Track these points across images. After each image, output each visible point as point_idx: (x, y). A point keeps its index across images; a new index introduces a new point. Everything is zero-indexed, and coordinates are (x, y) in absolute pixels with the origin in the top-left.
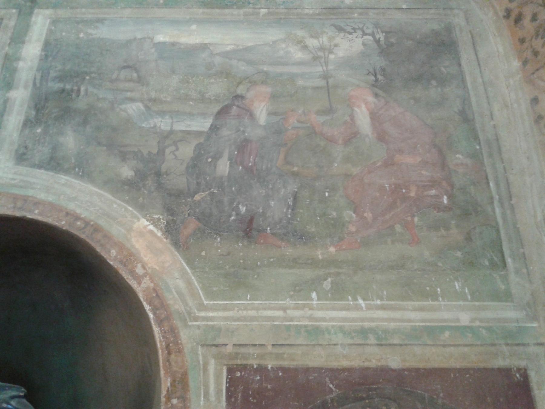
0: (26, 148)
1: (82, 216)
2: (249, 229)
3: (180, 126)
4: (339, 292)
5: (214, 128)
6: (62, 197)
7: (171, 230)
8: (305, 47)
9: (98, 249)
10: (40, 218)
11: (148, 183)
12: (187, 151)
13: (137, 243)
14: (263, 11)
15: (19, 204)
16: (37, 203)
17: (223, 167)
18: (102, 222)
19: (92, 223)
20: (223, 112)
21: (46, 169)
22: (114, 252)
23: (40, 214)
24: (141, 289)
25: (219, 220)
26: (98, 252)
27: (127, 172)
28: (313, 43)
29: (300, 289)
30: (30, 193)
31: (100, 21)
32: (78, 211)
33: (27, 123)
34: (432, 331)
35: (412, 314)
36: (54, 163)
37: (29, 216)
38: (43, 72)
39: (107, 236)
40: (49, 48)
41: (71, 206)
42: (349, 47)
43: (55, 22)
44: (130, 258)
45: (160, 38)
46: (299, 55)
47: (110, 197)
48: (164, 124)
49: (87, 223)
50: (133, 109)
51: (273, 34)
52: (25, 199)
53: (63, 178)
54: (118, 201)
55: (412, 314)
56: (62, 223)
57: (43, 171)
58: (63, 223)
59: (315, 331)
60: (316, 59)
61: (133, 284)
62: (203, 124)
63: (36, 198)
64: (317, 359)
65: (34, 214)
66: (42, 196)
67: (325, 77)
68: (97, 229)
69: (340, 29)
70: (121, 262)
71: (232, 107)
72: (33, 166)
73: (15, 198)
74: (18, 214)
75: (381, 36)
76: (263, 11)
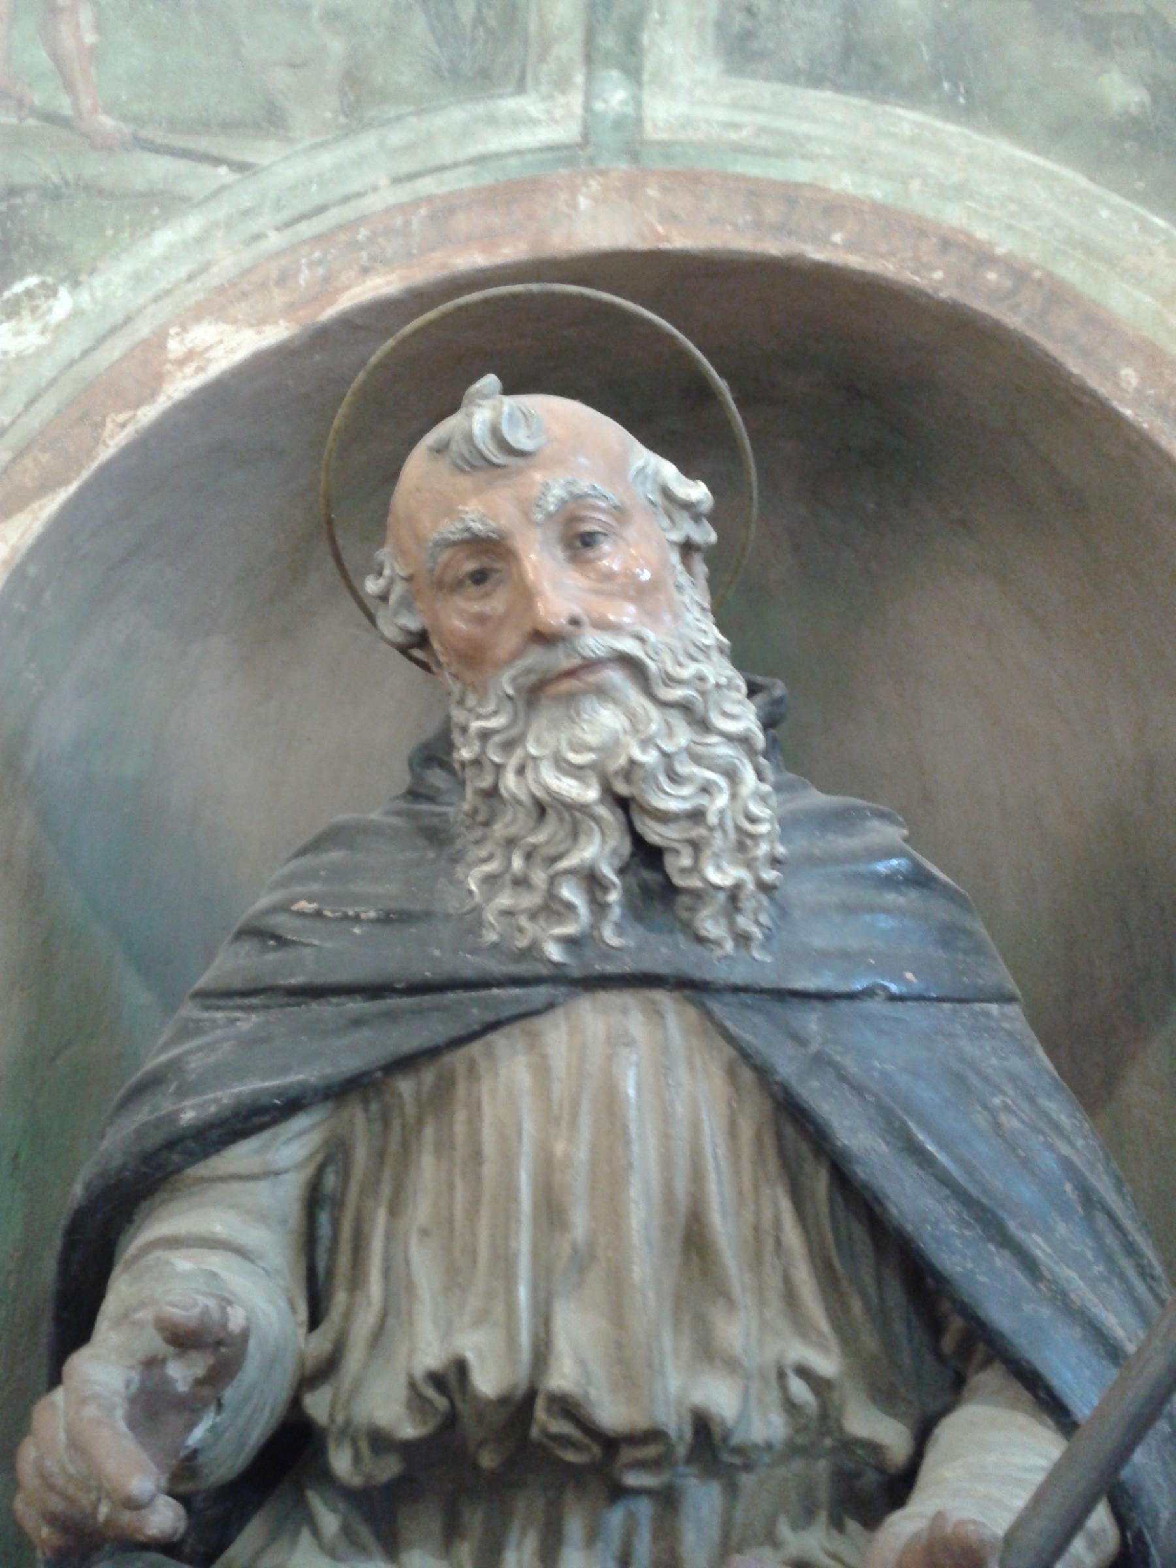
0: (750, 12)
1: (1000, 251)
6: (915, 185)
9: (1075, 366)
10: (855, 261)
15: (772, 213)
16: (835, 209)
18: (1070, 272)
19: (1037, 274)
21: (838, 88)
22: (1130, 376)
23: (851, 246)
26: (1071, 375)
30: (801, 172)
32: (982, 233)
37: (816, 254)
39: (1096, 320)
41: (954, 216)
47: (1083, 182)
49: (1020, 274)
52: (790, 194)
53: (907, 118)
54: (1116, 199)
56: (935, 279)
57: (828, 94)
58: (938, 275)
63: (826, 190)
65: (832, 249)
66: (845, 183)
68: (1057, 295)
70: (1161, 408)
72: (792, 76)
73: (755, 192)
74: (774, 248)
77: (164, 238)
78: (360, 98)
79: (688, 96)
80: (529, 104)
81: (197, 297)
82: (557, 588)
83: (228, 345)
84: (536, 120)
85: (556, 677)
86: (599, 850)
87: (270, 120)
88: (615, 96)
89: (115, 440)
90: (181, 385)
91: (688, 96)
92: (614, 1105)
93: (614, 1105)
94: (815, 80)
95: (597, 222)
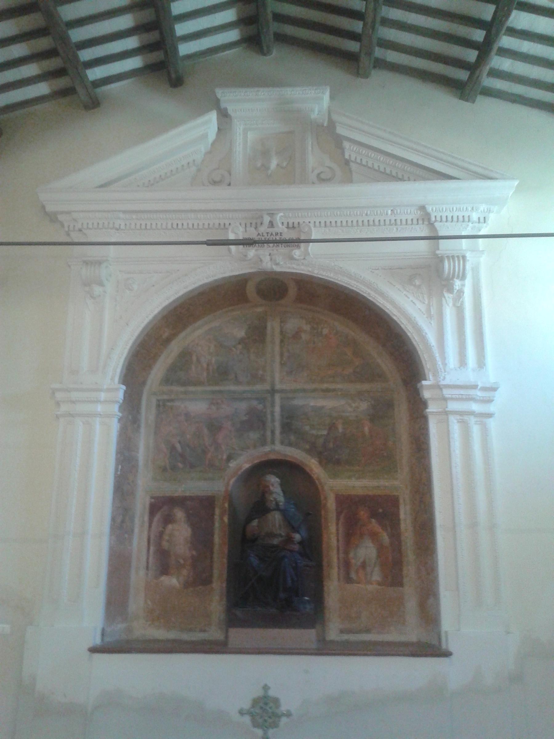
2: (338, 462)
3: (320, 433)
4: (358, 478)
5: (328, 434)
7: (320, 463)
8: (351, 407)
11: (312, 450)
12: (321, 441)
13: (313, 466)
14: (340, 393)
17: (331, 445)
20: (330, 429)
24: (315, 477)
25: (330, 458)
27: (308, 447)
28: (354, 405)
29: (350, 477)
31: (295, 398)
33: (282, 433)
34: (378, 487)
35: (375, 483)
36: (290, 445)
38: (282, 416)
40: (282, 408)
42: (364, 406)
43: (282, 398)
44: (311, 470)
45: (312, 404)
46: (350, 409)
48: (314, 432)
50: (307, 428)
51: (342, 402)
55: (375, 483)
59: (354, 487)
60: (354, 410)
61: (313, 475)
62: (325, 432)
64: (353, 493)
67: (357, 416)
69: (361, 400)
71: (332, 427)
75: (373, 402)
76: (340, 393)
77: (242, 457)
78: (255, 447)
79: (278, 447)
80: (267, 447)
81: (243, 462)
82: (271, 488)
83: (247, 466)
84: (267, 449)
85: (271, 493)
86: (274, 503)
87: (249, 448)
88: (273, 447)
89: (240, 473)
90: (244, 469)
91: (278, 447)
92: (276, 517)
93: (276, 517)
94: (287, 446)
95: (272, 457)
